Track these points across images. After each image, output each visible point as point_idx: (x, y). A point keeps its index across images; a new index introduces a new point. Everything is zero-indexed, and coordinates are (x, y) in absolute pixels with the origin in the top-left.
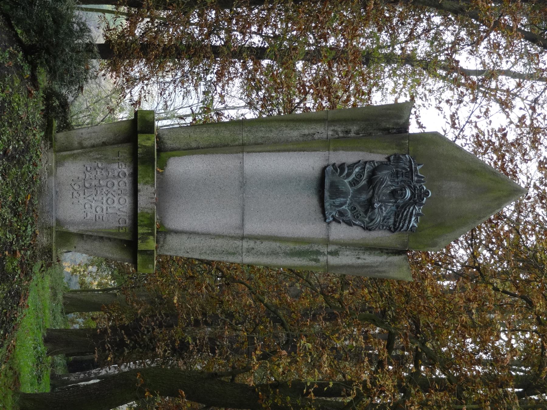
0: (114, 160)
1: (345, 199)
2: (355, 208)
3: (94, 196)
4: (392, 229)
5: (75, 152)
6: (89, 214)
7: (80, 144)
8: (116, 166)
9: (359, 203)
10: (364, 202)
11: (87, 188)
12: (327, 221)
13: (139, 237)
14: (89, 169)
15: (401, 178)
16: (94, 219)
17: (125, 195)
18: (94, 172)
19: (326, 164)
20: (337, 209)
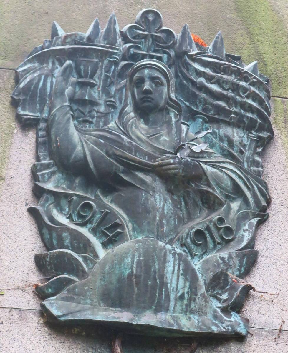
1: (170, 258)
2: (199, 233)
4: (265, 135)
9: (181, 221)
10: (176, 204)
12: (242, 330)
15: (96, 94)
19: (34, 322)
20: (203, 290)
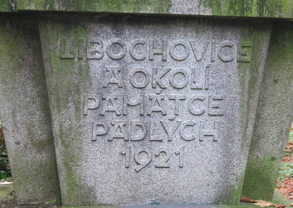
0: (80, 69)
3: (165, 120)
5: (60, 161)
6: (207, 131)
7: (40, 146)
8: (96, 67)
11: (147, 134)
13: (266, 15)
14: (101, 130)
16: (218, 119)
17: (164, 45)
18: (111, 118)
